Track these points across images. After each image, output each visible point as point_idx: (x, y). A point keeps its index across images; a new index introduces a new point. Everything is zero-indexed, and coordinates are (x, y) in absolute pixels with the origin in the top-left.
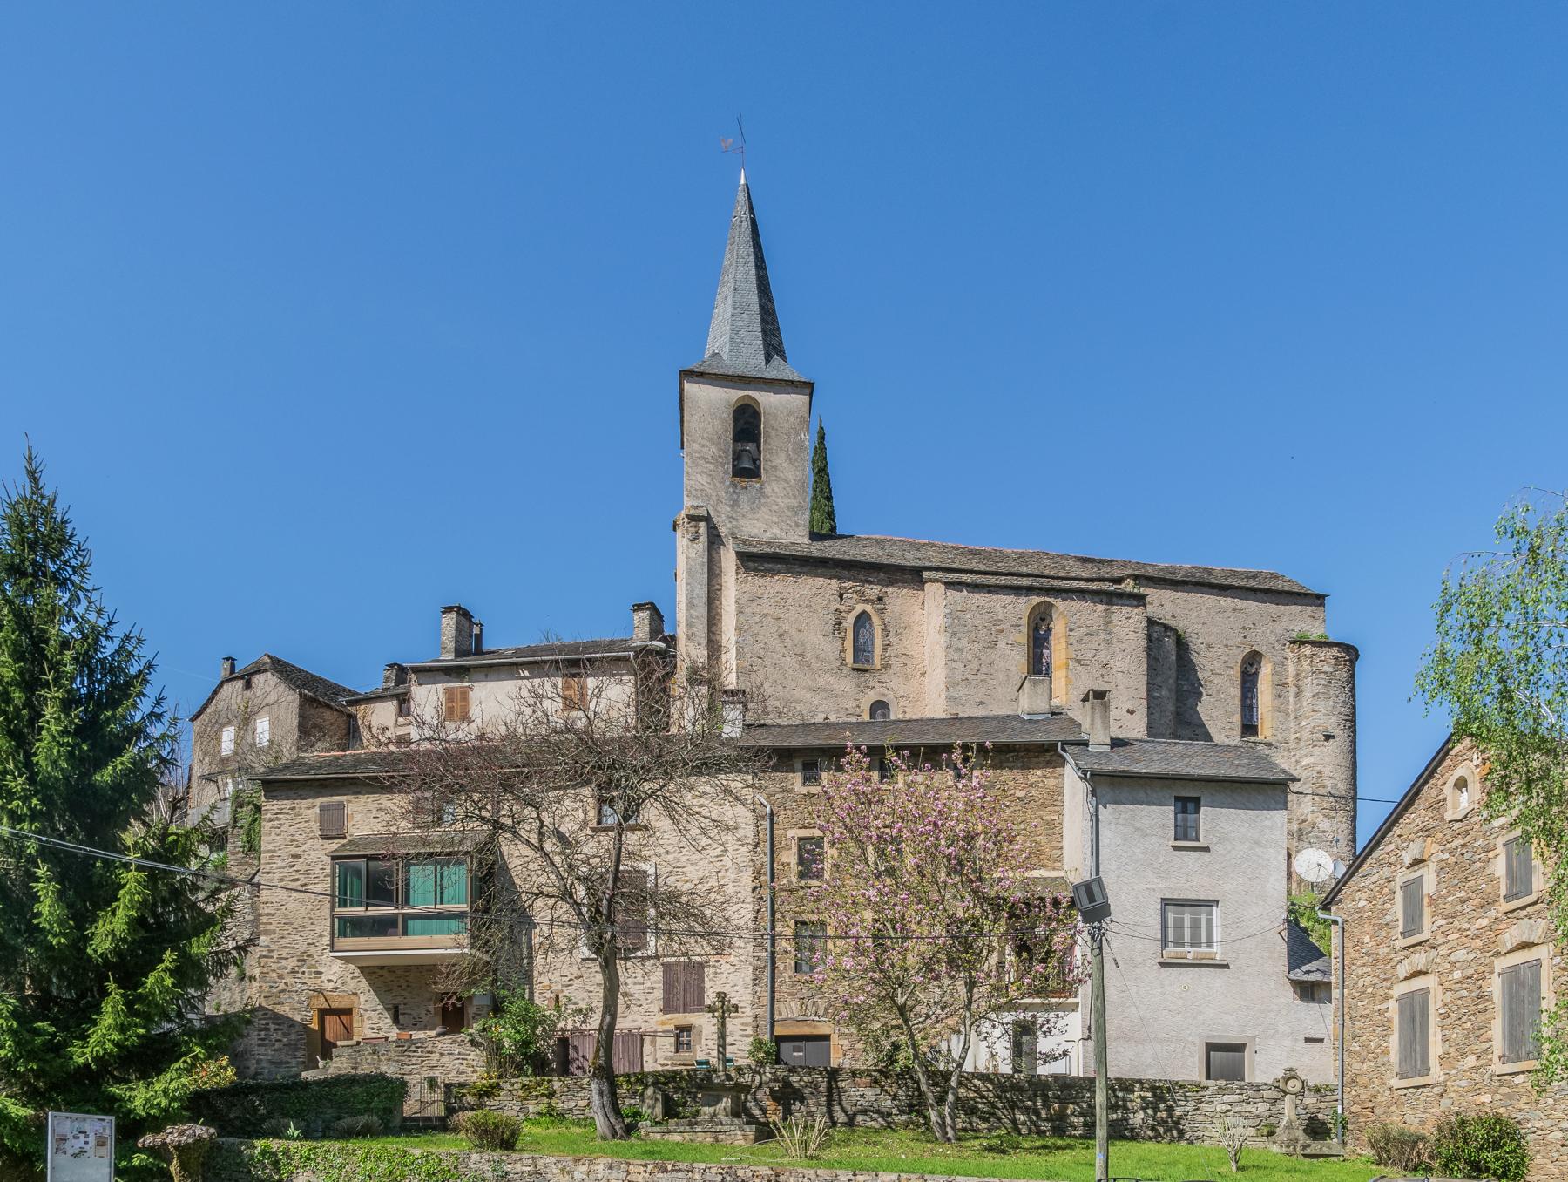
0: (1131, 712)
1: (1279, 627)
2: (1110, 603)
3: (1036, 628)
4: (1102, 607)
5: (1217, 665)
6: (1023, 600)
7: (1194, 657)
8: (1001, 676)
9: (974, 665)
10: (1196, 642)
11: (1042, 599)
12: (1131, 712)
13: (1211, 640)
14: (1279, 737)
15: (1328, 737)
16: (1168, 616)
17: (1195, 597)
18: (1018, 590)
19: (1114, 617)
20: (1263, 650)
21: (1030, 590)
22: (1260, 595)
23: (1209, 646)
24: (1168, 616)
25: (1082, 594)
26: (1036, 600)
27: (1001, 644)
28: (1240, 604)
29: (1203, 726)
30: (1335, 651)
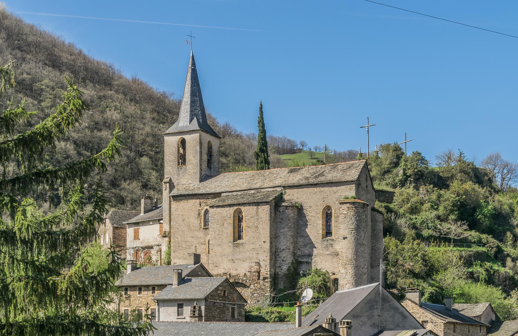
0: (264, 242)
1: (337, 195)
2: (258, 205)
3: (239, 217)
4: (255, 207)
5: (313, 213)
6: (232, 208)
7: (305, 212)
8: (225, 235)
9: (217, 233)
10: (305, 206)
11: (237, 207)
12: (264, 242)
13: (311, 204)
14: (336, 237)
15: (344, 238)
16: (295, 198)
17: (306, 189)
18: (230, 206)
19: (259, 210)
20: (331, 204)
21: (234, 205)
22: (330, 185)
23: (311, 207)
24: (295, 198)
25: (249, 204)
26: (235, 208)
27: (225, 224)
28: (322, 189)
29: (308, 236)
30: (348, 205)
